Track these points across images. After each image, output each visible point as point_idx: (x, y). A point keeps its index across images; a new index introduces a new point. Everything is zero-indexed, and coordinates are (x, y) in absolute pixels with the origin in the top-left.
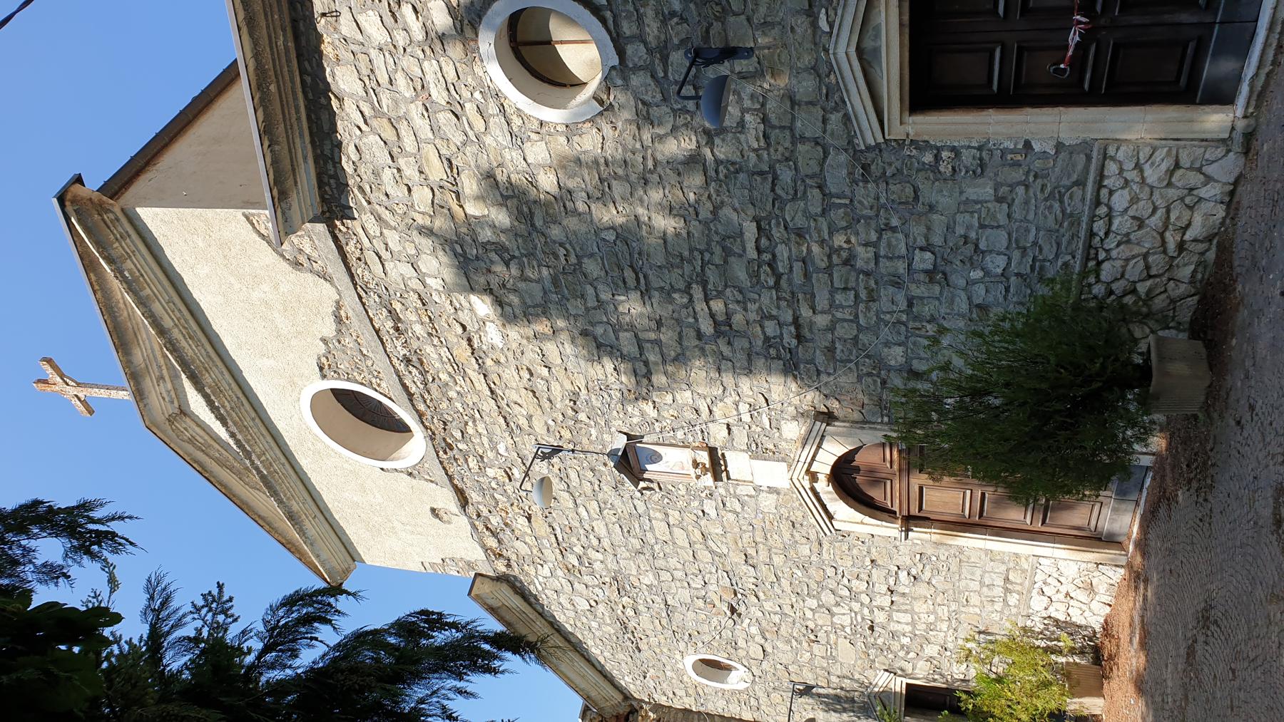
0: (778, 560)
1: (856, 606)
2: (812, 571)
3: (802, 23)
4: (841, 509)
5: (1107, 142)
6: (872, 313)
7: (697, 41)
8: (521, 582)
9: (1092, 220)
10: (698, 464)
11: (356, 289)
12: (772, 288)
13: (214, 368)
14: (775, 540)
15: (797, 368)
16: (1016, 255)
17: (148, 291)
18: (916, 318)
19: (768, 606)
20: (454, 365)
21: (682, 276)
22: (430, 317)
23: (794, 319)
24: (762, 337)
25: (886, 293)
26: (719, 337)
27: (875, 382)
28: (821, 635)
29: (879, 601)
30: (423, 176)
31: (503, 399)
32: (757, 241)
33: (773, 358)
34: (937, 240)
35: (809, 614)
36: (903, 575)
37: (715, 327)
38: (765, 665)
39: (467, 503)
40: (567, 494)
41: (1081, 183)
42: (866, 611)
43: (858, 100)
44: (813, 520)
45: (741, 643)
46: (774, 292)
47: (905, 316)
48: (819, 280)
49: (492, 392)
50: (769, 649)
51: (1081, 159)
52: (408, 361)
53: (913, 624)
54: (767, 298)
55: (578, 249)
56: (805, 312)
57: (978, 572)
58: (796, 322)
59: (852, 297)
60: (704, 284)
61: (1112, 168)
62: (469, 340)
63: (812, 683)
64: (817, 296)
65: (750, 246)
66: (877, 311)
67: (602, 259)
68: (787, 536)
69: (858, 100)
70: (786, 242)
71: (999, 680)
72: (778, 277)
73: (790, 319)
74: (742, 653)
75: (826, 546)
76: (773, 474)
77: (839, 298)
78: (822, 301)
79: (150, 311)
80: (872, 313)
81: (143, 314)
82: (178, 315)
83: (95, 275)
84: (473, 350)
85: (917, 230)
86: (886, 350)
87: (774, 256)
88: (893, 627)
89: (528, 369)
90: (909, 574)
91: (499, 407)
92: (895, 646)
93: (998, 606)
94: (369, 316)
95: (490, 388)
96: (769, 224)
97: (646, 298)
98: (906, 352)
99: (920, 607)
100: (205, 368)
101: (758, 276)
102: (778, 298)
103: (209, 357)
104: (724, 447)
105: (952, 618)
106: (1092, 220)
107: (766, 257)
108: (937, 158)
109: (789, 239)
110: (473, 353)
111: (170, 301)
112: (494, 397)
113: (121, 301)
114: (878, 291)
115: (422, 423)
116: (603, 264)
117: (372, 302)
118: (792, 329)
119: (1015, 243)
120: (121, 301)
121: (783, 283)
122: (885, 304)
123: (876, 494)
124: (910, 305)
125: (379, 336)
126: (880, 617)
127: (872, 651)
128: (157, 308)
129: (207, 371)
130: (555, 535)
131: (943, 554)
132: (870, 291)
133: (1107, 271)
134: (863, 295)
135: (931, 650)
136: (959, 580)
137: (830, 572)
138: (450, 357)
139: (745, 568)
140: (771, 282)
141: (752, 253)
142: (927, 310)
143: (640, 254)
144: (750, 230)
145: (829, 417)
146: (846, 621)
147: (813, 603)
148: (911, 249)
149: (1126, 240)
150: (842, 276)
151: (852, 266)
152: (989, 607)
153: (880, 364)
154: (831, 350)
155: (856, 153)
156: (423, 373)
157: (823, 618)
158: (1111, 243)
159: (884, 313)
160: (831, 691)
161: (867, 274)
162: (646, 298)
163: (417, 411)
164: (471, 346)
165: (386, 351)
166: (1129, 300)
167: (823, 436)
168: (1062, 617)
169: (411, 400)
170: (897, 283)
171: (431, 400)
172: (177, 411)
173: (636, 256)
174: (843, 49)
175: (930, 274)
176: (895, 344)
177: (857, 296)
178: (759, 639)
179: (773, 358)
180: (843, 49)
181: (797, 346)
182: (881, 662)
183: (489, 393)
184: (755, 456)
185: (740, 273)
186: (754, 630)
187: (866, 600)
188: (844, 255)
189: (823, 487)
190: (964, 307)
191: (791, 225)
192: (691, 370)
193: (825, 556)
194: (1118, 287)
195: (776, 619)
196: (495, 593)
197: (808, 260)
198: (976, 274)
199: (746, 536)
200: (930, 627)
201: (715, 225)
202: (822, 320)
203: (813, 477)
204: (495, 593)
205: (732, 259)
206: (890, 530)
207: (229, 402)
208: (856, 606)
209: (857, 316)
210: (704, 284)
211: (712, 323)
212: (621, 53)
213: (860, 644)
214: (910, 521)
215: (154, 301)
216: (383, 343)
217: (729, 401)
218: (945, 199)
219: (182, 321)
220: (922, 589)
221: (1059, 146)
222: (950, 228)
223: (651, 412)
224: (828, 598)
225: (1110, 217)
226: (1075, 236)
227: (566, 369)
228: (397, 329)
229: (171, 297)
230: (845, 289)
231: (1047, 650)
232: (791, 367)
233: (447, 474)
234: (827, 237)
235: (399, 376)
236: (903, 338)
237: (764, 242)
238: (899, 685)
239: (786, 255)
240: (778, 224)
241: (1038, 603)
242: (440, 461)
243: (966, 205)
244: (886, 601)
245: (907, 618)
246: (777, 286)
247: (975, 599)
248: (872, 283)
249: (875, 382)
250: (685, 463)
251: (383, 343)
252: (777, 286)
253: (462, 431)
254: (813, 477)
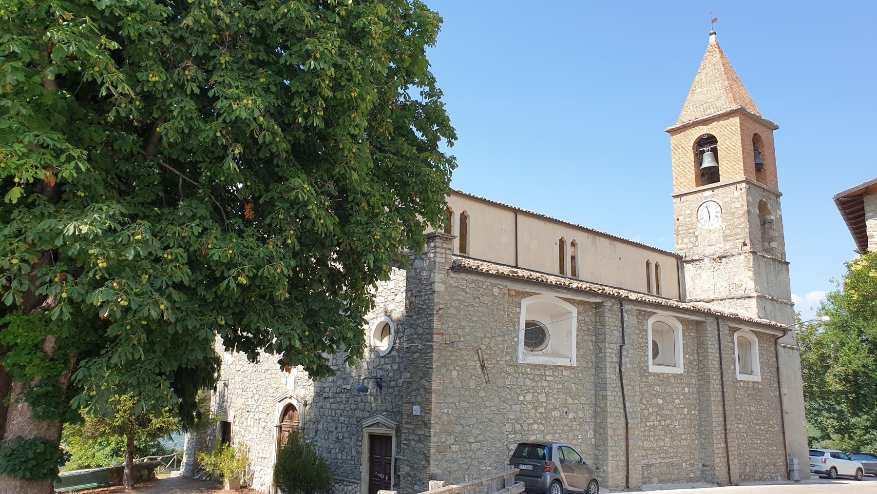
0: (267, 381)
1: (255, 407)
2: (264, 393)
3: (384, 408)
4: (281, 406)
5: (360, 484)
7: (384, 379)
9: (347, 481)
14: (272, 381)
16: (341, 461)
19: (253, 374)
25: (333, 424)
28: (244, 393)
29: (257, 415)
34: (345, 440)
35: (251, 390)
36: (265, 424)
38: (234, 370)
41: (355, 478)
42: (253, 410)
43: (371, 421)
44: (279, 395)
45: (240, 363)
50: (240, 373)
51: (358, 478)
53: (250, 426)
54: (334, 389)
56: (331, 401)
57: (266, 449)
58: (328, 397)
61: (356, 485)
63: (229, 387)
68: (274, 385)
69: (371, 421)
71: (233, 456)
74: (237, 362)
75: (272, 398)
76: (291, 386)
77: (333, 411)
78: (333, 406)
85: (346, 435)
88: (249, 419)
92: (243, 419)
93: (257, 455)
99: (256, 429)
105: (252, 439)
106: (347, 481)
108: (361, 441)
119: (344, 461)
123: (287, 417)
126: (252, 415)
127: (240, 411)
131: (271, 438)
133: (337, 485)
135: (242, 432)
137: (265, 399)
139: (264, 369)
142: (330, 436)
144: (348, 387)
145: (305, 405)
146: (250, 403)
147: (255, 392)
148: (343, 433)
149: (343, 490)
152: (257, 452)
153: (319, 422)
154: (322, 408)
155: (361, 419)
157: (250, 395)
158: (342, 486)
160: (226, 394)
166: (331, 491)
168: (255, 476)
170: (336, 428)
174: (380, 418)
175: (337, 438)
178: (242, 370)
180: (380, 418)
182: (238, 414)
184: (295, 379)
185: (340, 382)
186: (245, 368)
187: (257, 410)
189: (287, 401)
190: (331, 447)
193: (269, 398)
194: (333, 489)
195: (249, 377)
198: (337, 451)
199: (273, 371)
200: (250, 432)
203: (290, 398)
206: (277, 421)
208: (255, 407)
212: (383, 357)
213: (243, 407)
214: (280, 428)
218: (352, 443)
220: (261, 430)
221: (361, 472)
222: (347, 444)
224: (256, 397)
225: (347, 486)
226: (345, 477)
231: (245, 471)
238: (230, 419)
241: (258, 468)
243: (351, 449)
244: (257, 417)
245: (252, 424)
246: (337, 393)
247: (259, 447)
252: (337, 393)
254: (290, 398)
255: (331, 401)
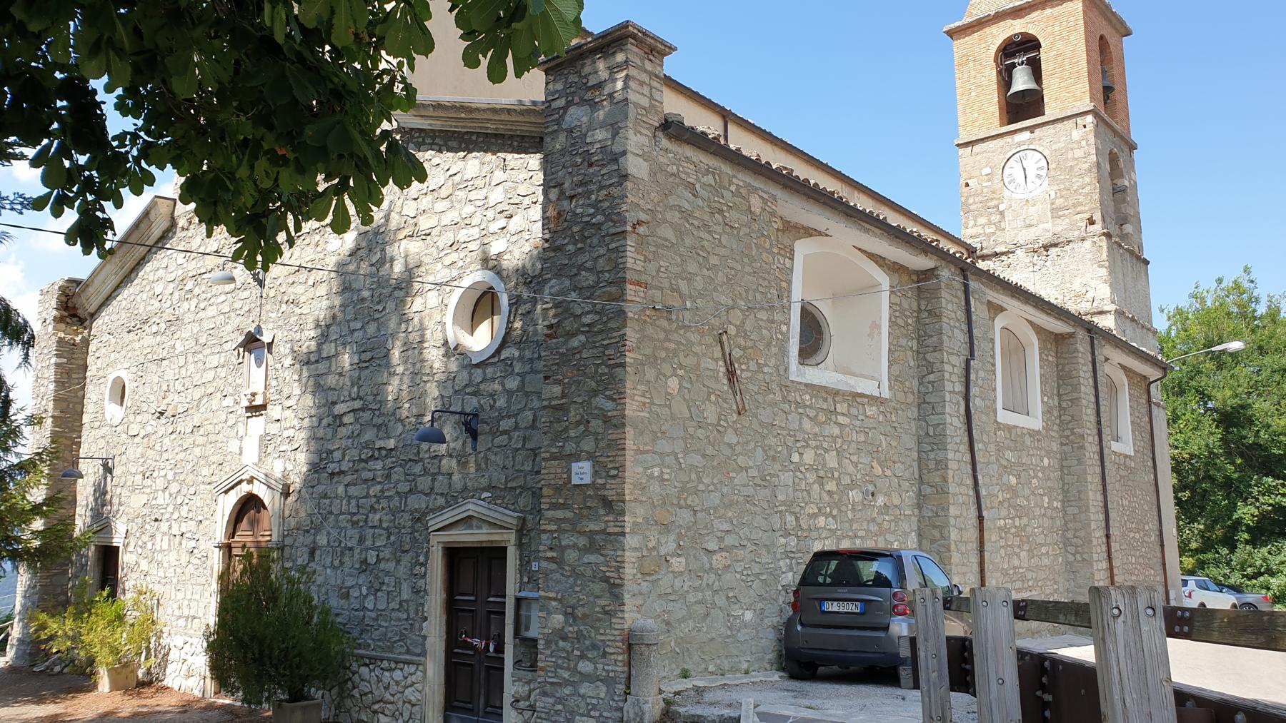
0: (197, 451)
1: (170, 509)
2: (191, 477)
3: (484, 482)
4: (233, 498)
5: (424, 664)
7: (482, 416)
8: (172, 238)
9: (389, 660)
14: (210, 450)
15: (316, 472)
16: (373, 615)
19: (166, 441)
25: (355, 533)
28: (148, 482)
29: (175, 526)
34: (382, 566)
35: (163, 473)
36: (193, 544)
38: (124, 436)
41: (408, 652)
42: (167, 516)
43: (449, 516)
44: (223, 478)
45: (139, 418)
50: (137, 440)
51: (418, 651)
53: (162, 551)
54: (354, 453)
56: (348, 479)
57: (197, 597)
58: (341, 472)
60: (363, 409)
61: (412, 669)
63: (115, 473)
68: (213, 459)
69: (449, 516)
71: (120, 618)
74: (132, 418)
75: (209, 488)
76: (251, 453)
77: (354, 502)
78: (353, 491)
85: (386, 553)
87: (377, 459)
88: (159, 536)
92: (145, 538)
93: (177, 613)
99: (173, 556)
105: (165, 581)
106: (389, 660)
108: (422, 565)
118: (337, 470)
119: (380, 614)
121: (363, 465)
122: (350, 532)
123: (244, 524)
126: (164, 526)
127: (140, 521)
131: (207, 572)
133: (364, 670)
134: (355, 518)
135: (144, 565)
137: (192, 490)
139: (190, 425)
140: (363, 456)
142: (346, 559)
144: (391, 443)
145: (286, 493)
146: (160, 501)
147: (170, 476)
148: (378, 549)
149: (379, 680)
152: (175, 606)
153: (317, 529)
154: (325, 496)
155: (425, 514)
157: (160, 483)
158: (378, 672)
160: (109, 488)
161: (366, 521)
166: (350, 685)
168: (170, 658)
170: (361, 540)
174: (472, 507)
175: (364, 562)
177: (355, 514)
178: (143, 433)
180: (472, 507)
182: (134, 527)
184: (261, 438)
185: (369, 435)
186: (149, 429)
187: (175, 516)
188: (376, 506)
189: (245, 488)
190: (348, 584)
193: (202, 487)
194: (356, 678)
195: (158, 447)
198: (364, 591)
199: (211, 428)
200: (160, 564)
203: (250, 481)
206: (219, 534)
208: (170, 509)
209: (344, 514)
210: (363, 409)
212: (478, 365)
213: (145, 511)
214: (227, 549)
218: (402, 570)
220: (185, 557)
221: (425, 637)
222: (388, 573)
224: (174, 488)
225: (390, 670)
226: (383, 650)
230: (358, 507)
231: (148, 649)
232: (316, 468)
237: (384, 452)
238: (117, 541)
240: (393, 463)
241: (177, 641)
243: (398, 583)
244: (175, 531)
245: (165, 547)
246: (361, 460)
247: (180, 595)
248: (361, 524)
252: (361, 460)
254: (250, 481)
255: (348, 479)
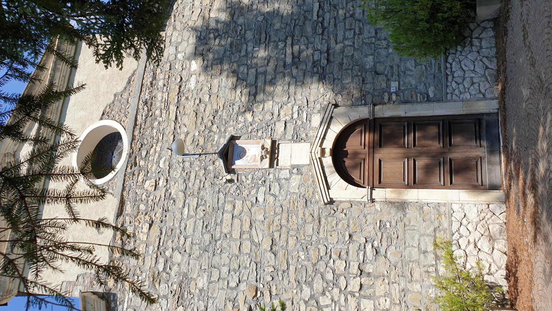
4: (335, 179)
6: (360, 40)
10: (264, 148)
11: (147, 62)
12: (320, 34)
13: (55, 114)
15: (325, 78)
17: (60, 67)
18: (379, 40)
20: (166, 103)
21: (285, 33)
22: (169, 76)
23: (327, 50)
24: (312, 61)
25: (367, 28)
26: (293, 65)
27: (359, 79)
30: (201, 4)
31: (179, 123)
32: (318, 12)
33: (315, 73)
37: (292, 59)
39: (121, 214)
40: (183, 194)
46: (321, 36)
47: (374, 39)
48: (340, 25)
49: (176, 118)
52: (146, 103)
55: (246, 26)
59: (353, 33)
60: (293, 37)
62: (180, 87)
64: (338, 35)
65: (315, 14)
66: (362, 39)
67: (255, 30)
70: (329, 12)
72: (324, 29)
73: (325, 49)
77: (347, 33)
79: (54, 75)
80: (360, 40)
81: (50, 74)
82: (62, 83)
83: (46, 58)
84: (179, 92)
86: (365, 59)
87: (323, 19)
89: (200, 99)
90: (372, 247)
91: (175, 129)
94: (144, 76)
95: (176, 115)
96: (324, 4)
97: (267, 47)
98: (374, 59)
100: (52, 112)
101: (316, 29)
102: (322, 39)
103: (58, 108)
104: (279, 140)
107: (320, 19)
109: (330, 10)
110: (178, 94)
111: (64, 77)
112: (176, 122)
113: (44, 75)
114: (363, 28)
115: (131, 144)
116: (254, 32)
117: (150, 68)
118: (326, 55)
120: (44, 75)
121: (325, 33)
122: (366, 34)
124: (376, 33)
125: (141, 88)
128: (58, 75)
129: (51, 113)
130: (160, 239)
132: (360, 29)
134: (357, 32)
136: (405, 249)
138: (167, 98)
140: (320, 32)
141: (315, 17)
143: (270, 25)
150: (349, 22)
151: (354, 18)
156: (149, 111)
159: (365, 39)
161: (360, 21)
162: (267, 47)
163: (133, 135)
164: (180, 89)
165: (140, 96)
167: (332, 117)
169: (134, 128)
171: (144, 129)
172: (12, 153)
173: (269, 26)
176: (369, 55)
177: (355, 32)
179: (315, 73)
181: (326, 65)
183: (174, 119)
188: (351, 13)
191: (332, 3)
192: (276, 87)
196: (96, 304)
197: (337, 18)
201: (303, 7)
202: (339, 46)
204: (96, 304)
205: (307, 22)
207: (47, 134)
209: (354, 43)
210: (293, 37)
211: (292, 57)
215: (59, 72)
216: (141, 92)
217: (289, 105)
219: (61, 87)
223: (250, 118)
227: (218, 96)
228: (151, 84)
229: (66, 75)
230: (350, 29)
232: (322, 78)
233: (123, 185)
234: (345, 6)
235: (137, 112)
236: (373, 52)
237: (321, 11)
239: (328, 17)
240: (327, 3)
242: (125, 174)
248: (361, 24)
249: (359, 79)
250: (257, 155)
251: (141, 92)
253: (147, 152)
255: (333, 42)
